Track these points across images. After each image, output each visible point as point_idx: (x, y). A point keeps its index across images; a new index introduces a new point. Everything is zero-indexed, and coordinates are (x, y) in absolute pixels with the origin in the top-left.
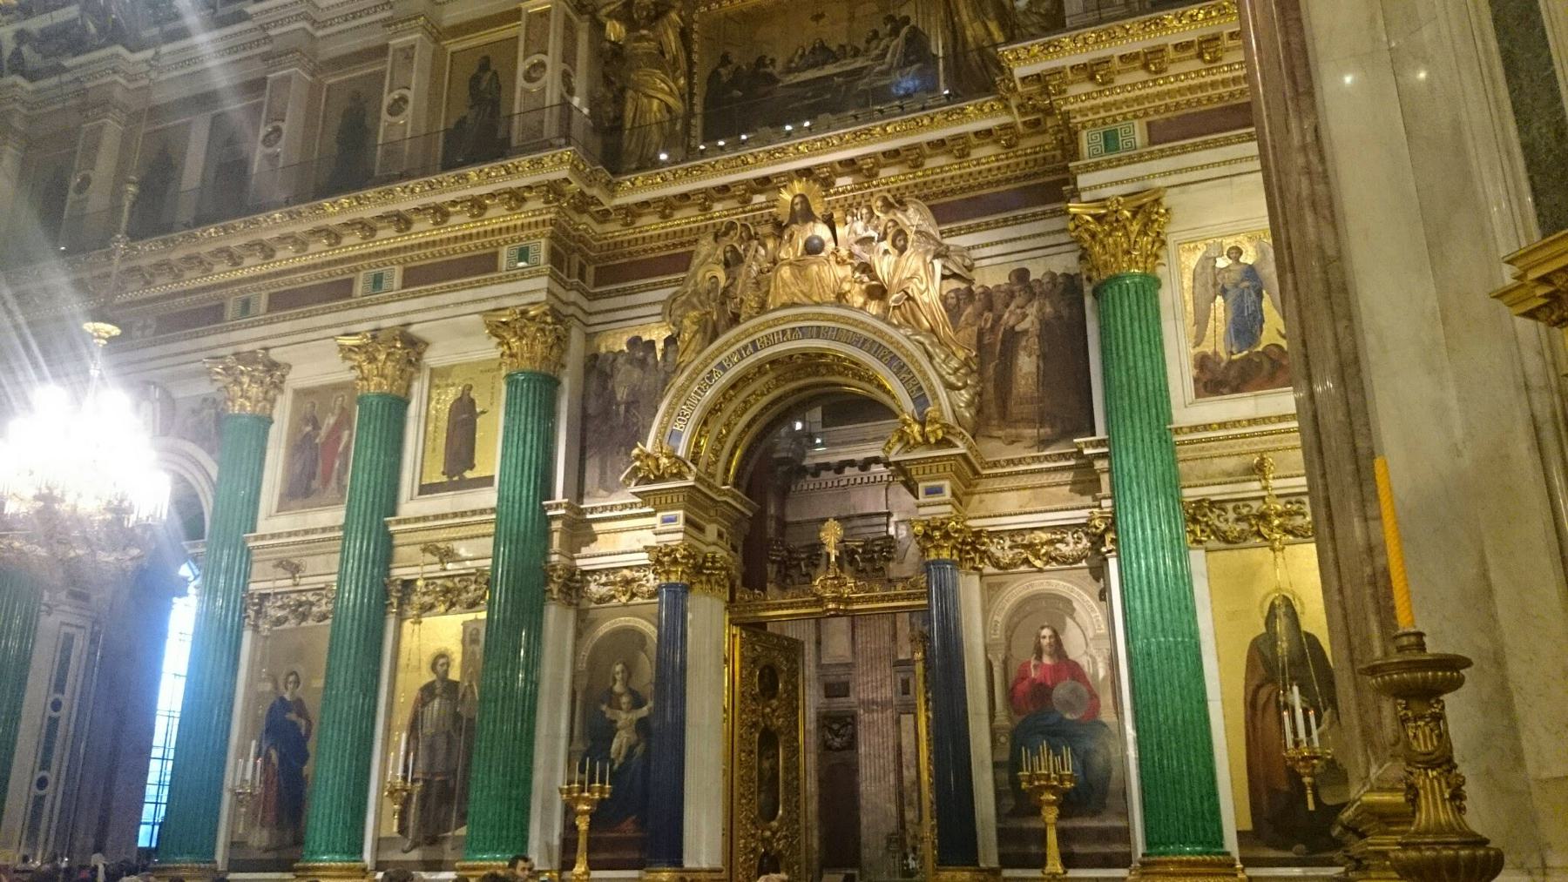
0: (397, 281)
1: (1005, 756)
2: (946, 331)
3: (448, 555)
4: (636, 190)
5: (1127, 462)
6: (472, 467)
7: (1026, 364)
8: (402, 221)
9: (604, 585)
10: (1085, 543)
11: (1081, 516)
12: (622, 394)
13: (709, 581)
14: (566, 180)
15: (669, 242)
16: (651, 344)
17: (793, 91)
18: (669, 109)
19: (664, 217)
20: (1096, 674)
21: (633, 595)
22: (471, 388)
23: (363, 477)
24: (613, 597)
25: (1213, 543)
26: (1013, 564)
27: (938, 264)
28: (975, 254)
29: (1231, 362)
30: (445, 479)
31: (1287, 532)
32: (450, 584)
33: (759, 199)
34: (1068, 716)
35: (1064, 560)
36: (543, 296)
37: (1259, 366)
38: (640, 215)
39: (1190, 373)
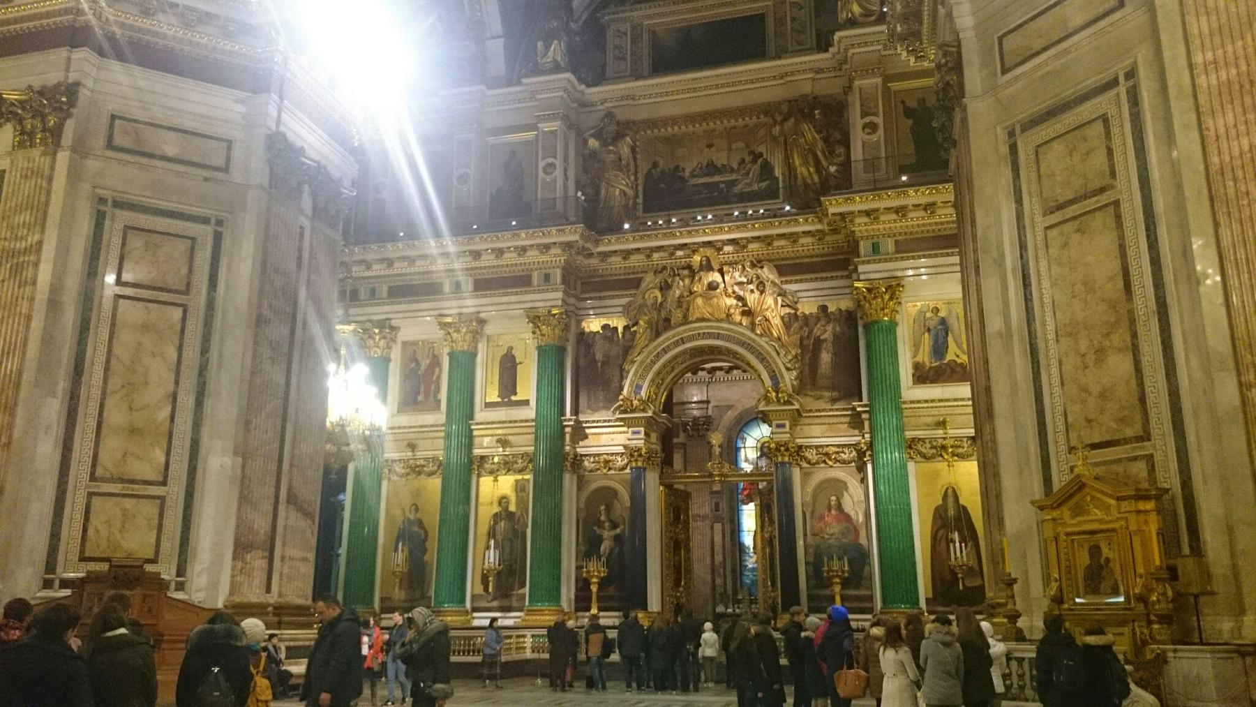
1: (811, 559)
2: (784, 338)
4: (610, 244)
5: (880, 417)
6: (515, 394)
7: (826, 357)
10: (854, 453)
11: (854, 440)
12: (599, 356)
16: (616, 329)
18: (625, 193)
19: (625, 258)
23: (456, 398)
25: (919, 458)
26: (818, 463)
27: (780, 299)
28: (800, 295)
33: (680, 253)
35: (844, 462)
36: (560, 303)
37: (945, 371)
39: (910, 371)
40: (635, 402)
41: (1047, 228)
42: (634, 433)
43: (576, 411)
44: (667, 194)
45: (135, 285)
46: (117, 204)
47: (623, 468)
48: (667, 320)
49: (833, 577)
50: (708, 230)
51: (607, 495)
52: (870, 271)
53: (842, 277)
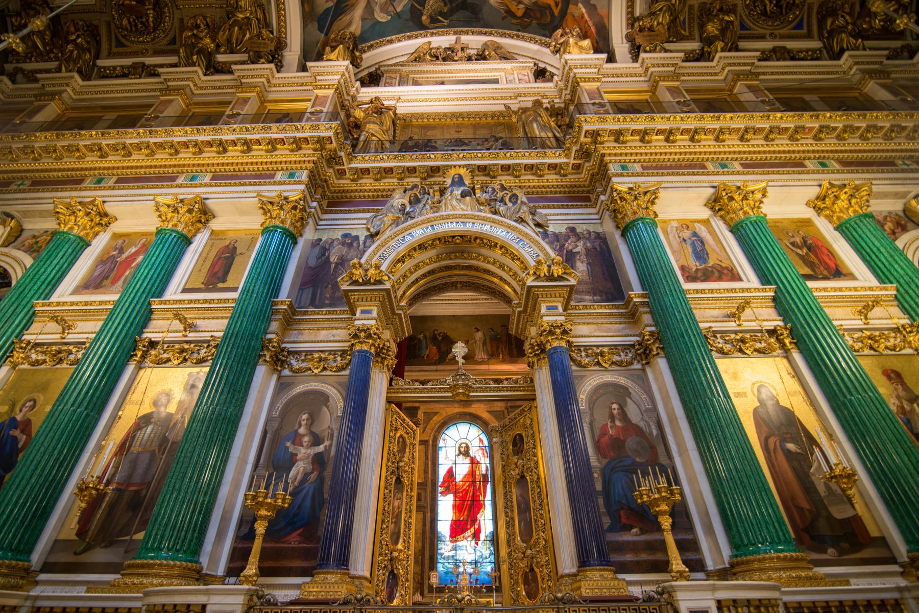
0: (207, 180)
3: (189, 327)
8: (223, 147)
9: (303, 361)
12: (333, 259)
13: (382, 363)
14: (330, 138)
15: (375, 194)
16: (357, 238)
20: (651, 433)
21: (324, 369)
24: (310, 369)
29: (697, 270)
31: (756, 350)
32: (186, 346)
34: (638, 459)
35: (619, 364)
38: (362, 178)
42: (363, 312)
47: (343, 369)
53: (587, 207)
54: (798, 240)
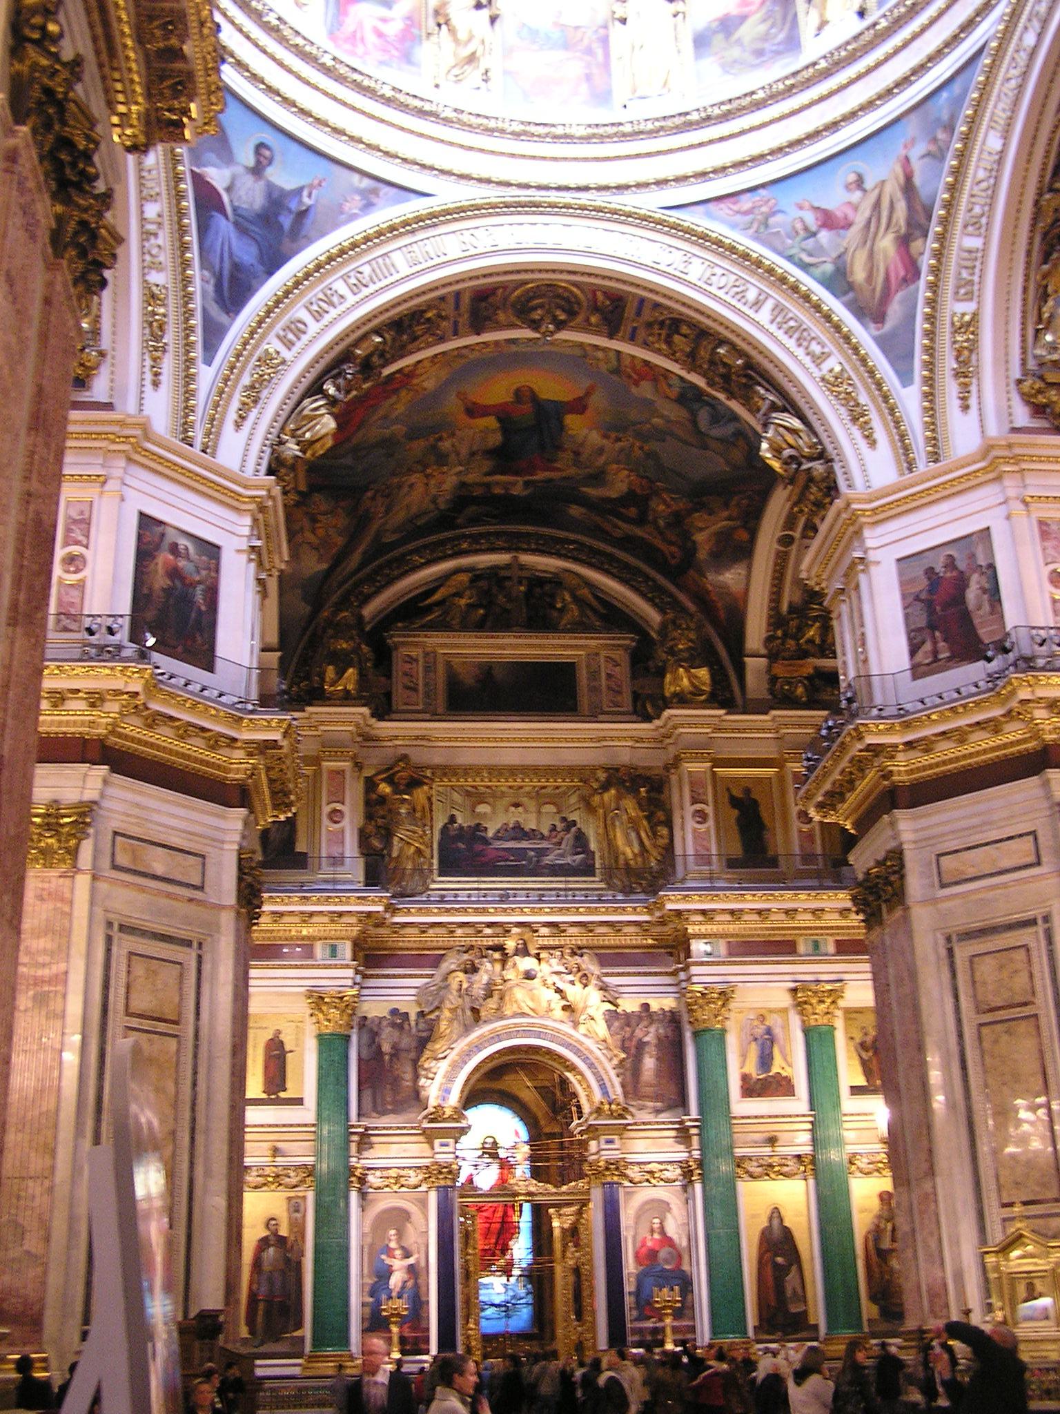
1: (633, 1289)
5: (712, 1133)
6: (285, 1090)
7: (649, 1063)
10: (679, 1171)
12: (386, 1048)
17: (501, 853)
22: (279, 1032)
30: (264, 1096)
33: (488, 931)
36: (350, 982)
40: (448, 1112)
41: (981, 1025)
43: (359, 1115)
44: (465, 853)
45: (140, 1016)
46: (122, 928)
48: (475, 1011)
49: (664, 1308)
50: (523, 906)
51: (399, 1218)
52: (702, 976)
53: (667, 974)
54: (869, 1039)
